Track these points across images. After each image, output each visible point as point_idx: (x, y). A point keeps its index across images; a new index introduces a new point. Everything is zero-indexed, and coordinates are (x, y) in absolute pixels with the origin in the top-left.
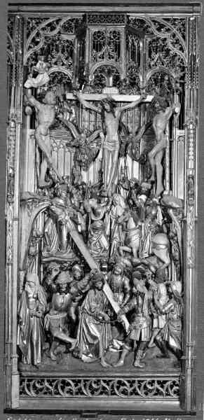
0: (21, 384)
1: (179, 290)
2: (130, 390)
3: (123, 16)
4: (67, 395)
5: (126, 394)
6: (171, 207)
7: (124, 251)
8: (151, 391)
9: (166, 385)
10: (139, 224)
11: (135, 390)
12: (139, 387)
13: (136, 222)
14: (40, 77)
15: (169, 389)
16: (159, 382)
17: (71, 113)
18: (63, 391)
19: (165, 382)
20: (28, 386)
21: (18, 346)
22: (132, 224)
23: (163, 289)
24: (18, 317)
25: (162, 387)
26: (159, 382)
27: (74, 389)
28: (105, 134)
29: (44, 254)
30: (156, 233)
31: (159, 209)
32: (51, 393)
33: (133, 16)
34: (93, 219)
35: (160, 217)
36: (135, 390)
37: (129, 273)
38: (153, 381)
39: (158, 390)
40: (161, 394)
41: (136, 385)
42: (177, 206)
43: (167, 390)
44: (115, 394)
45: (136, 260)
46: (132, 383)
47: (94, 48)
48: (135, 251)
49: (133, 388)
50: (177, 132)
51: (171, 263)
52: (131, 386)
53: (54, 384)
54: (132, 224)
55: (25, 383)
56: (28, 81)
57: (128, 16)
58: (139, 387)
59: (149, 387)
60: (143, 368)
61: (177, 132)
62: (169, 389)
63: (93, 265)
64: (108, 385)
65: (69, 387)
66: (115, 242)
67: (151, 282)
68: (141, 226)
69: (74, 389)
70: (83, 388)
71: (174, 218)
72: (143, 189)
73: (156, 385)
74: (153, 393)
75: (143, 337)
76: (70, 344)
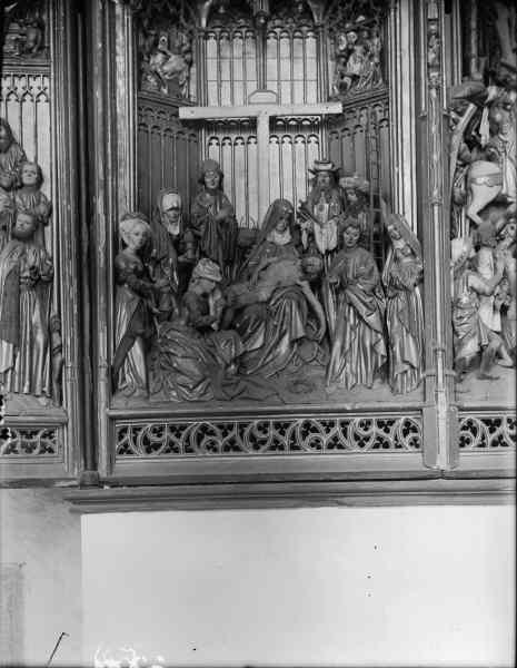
11: (335, 439)
18: (199, 444)
19: (391, 423)
59: (361, 432)
65: (213, 438)
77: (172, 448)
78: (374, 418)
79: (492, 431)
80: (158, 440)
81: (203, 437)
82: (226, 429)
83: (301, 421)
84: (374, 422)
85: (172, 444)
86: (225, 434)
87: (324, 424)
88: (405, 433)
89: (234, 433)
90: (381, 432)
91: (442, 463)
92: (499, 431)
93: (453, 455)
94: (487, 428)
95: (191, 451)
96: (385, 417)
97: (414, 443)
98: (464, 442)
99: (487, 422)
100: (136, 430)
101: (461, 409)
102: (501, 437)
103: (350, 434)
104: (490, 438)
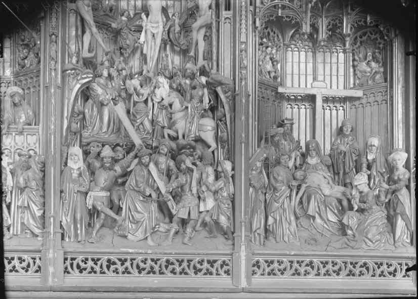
0: (65, 263)
2: (178, 269)
5: (175, 273)
6: (220, 84)
7: (169, 135)
8: (200, 270)
9: (216, 265)
10: (186, 104)
11: (183, 269)
12: (189, 266)
13: (181, 103)
15: (220, 269)
16: (209, 262)
18: (108, 269)
19: (215, 261)
20: (72, 265)
22: (177, 105)
23: (210, 170)
25: (212, 266)
26: (209, 262)
27: (121, 269)
28: (147, 16)
30: (203, 116)
31: (206, 90)
32: (95, 272)
34: (136, 100)
35: (206, 100)
37: (174, 155)
38: (203, 261)
39: (207, 270)
40: (211, 274)
41: (185, 264)
43: (217, 270)
44: (163, 273)
45: (181, 141)
50: (224, 14)
51: (217, 148)
52: (180, 265)
53: (99, 263)
54: (177, 105)
55: (68, 262)
58: (189, 266)
59: (199, 266)
61: (224, 14)
62: (220, 269)
63: (137, 141)
64: (156, 263)
66: (158, 128)
67: (198, 163)
68: (187, 108)
69: (121, 269)
70: (130, 267)
71: (222, 96)
72: (188, 71)
73: (206, 265)
74: (203, 272)
75: (191, 215)
77: (93, 271)
78: (205, 258)
79: (269, 266)
81: (110, 267)
82: (123, 262)
83: (165, 258)
85: (92, 268)
86: (122, 264)
87: (178, 261)
88: (222, 266)
89: (128, 264)
90: (209, 266)
91: (244, 284)
92: (272, 267)
93: (248, 279)
95: (104, 273)
97: (227, 272)
98: (254, 273)
99: (266, 262)
100: (73, 259)
101: (253, 254)
102: (273, 270)
104: (267, 270)
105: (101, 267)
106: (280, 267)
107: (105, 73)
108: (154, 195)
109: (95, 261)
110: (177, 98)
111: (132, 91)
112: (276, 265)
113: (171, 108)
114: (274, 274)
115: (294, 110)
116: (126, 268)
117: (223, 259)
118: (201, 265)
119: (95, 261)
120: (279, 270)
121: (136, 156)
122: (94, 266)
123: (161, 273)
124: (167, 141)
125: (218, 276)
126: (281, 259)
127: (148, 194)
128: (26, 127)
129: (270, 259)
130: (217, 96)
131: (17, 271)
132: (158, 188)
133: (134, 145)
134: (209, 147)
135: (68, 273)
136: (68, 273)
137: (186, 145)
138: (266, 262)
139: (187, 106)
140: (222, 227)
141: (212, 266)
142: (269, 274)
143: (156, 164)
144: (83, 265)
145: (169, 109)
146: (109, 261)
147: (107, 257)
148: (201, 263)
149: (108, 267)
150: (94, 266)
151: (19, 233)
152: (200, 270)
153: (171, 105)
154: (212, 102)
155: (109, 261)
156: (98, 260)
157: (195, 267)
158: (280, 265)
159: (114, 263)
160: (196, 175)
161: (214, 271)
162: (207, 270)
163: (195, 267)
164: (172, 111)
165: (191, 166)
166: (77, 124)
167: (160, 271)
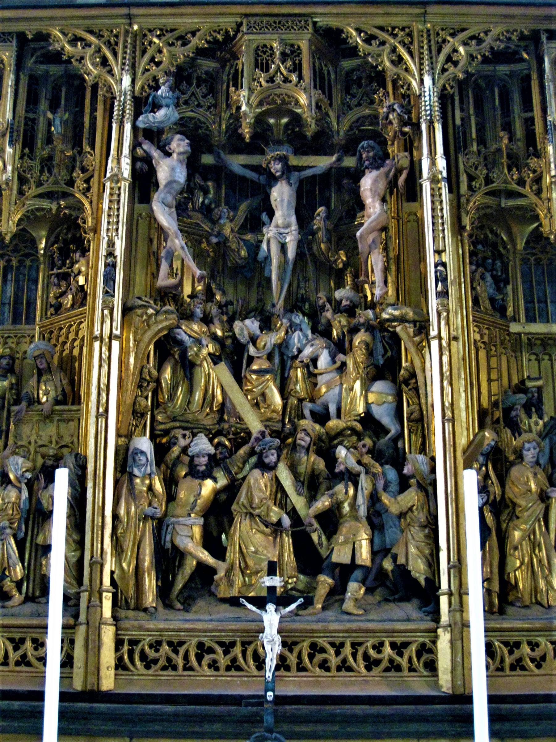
0: (117, 649)
1: (425, 469)
2: (334, 661)
3: (306, 21)
4: (208, 672)
5: (328, 669)
8: (378, 662)
10: (341, 357)
11: (344, 661)
14: (161, 114)
17: (206, 192)
19: (406, 645)
20: (131, 653)
21: (112, 573)
22: (324, 361)
23: (392, 474)
24: (115, 517)
25: (401, 654)
27: (223, 661)
29: (159, 418)
32: (175, 668)
33: (321, 21)
36: (344, 661)
39: (391, 661)
41: (347, 650)
42: (417, 318)
44: (304, 669)
46: (338, 648)
47: (256, 66)
48: (332, 409)
49: (341, 657)
52: (338, 653)
54: (324, 361)
56: (141, 118)
57: (315, 23)
58: (354, 655)
59: (372, 653)
60: (362, 615)
64: (291, 651)
68: (344, 364)
69: (223, 661)
76: (214, 571)
77: (171, 665)
80: (156, 655)
81: (203, 657)
82: (227, 647)
84: (387, 644)
85: (169, 660)
88: (419, 654)
92: (517, 654)
94: (506, 651)
95: (191, 669)
96: (399, 640)
102: (520, 660)
103: (360, 656)
105: (186, 657)
106: (533, 654)
107: (199, 312)
108: (287, 521)
109: (175, 646)
110: (326, 348)
111: (243, 340)
112: (526, 649)
113: (316, 367)
114: (523, 668)
115: (543, 363)
116: (234, 660)
117: (421, 640)
118: (379, 652)
119: (175, 646)
120: (533, 660)
121: (252, 453)
122: (173, 656)
123: (301, 668)
124: (307, 423)
125: (412, 674)
126: (534, 639)
127: (274, 519)
128: (58, 408)
129: (513, 638)
130: (396, 339)
131: (29, 664)
132: (294, 509)
133: (249, 434)
134: (387, 432)
135: (125, 668)
136: (125, 668)
137: (344, 429)
138: (506, 644)
139: (344, 360)
140: (415, 581)
141: (401, 654)
142: (513, 668)
143: (293, 468)
144: (151, 654)
145: (311, 368)
146: (200, 645)
147: (196, 639)
148: (378, 647)
149: (199, 658)
150: (173, 656)
151: (38, 594)
152: (378, 662)
153: (314, 360)
154: (389, 354)
155: (200, 645)
156: (181, 644)
157: (366, 657)
158: (533, 650)
159: (211, 651)
160: (365, 482)
161: (404, 662)
162: (391, 661)
163: (366, 657)
164: (316, 371)
165: (352, 463)
166: (146, 398)
167: (298, 664)
